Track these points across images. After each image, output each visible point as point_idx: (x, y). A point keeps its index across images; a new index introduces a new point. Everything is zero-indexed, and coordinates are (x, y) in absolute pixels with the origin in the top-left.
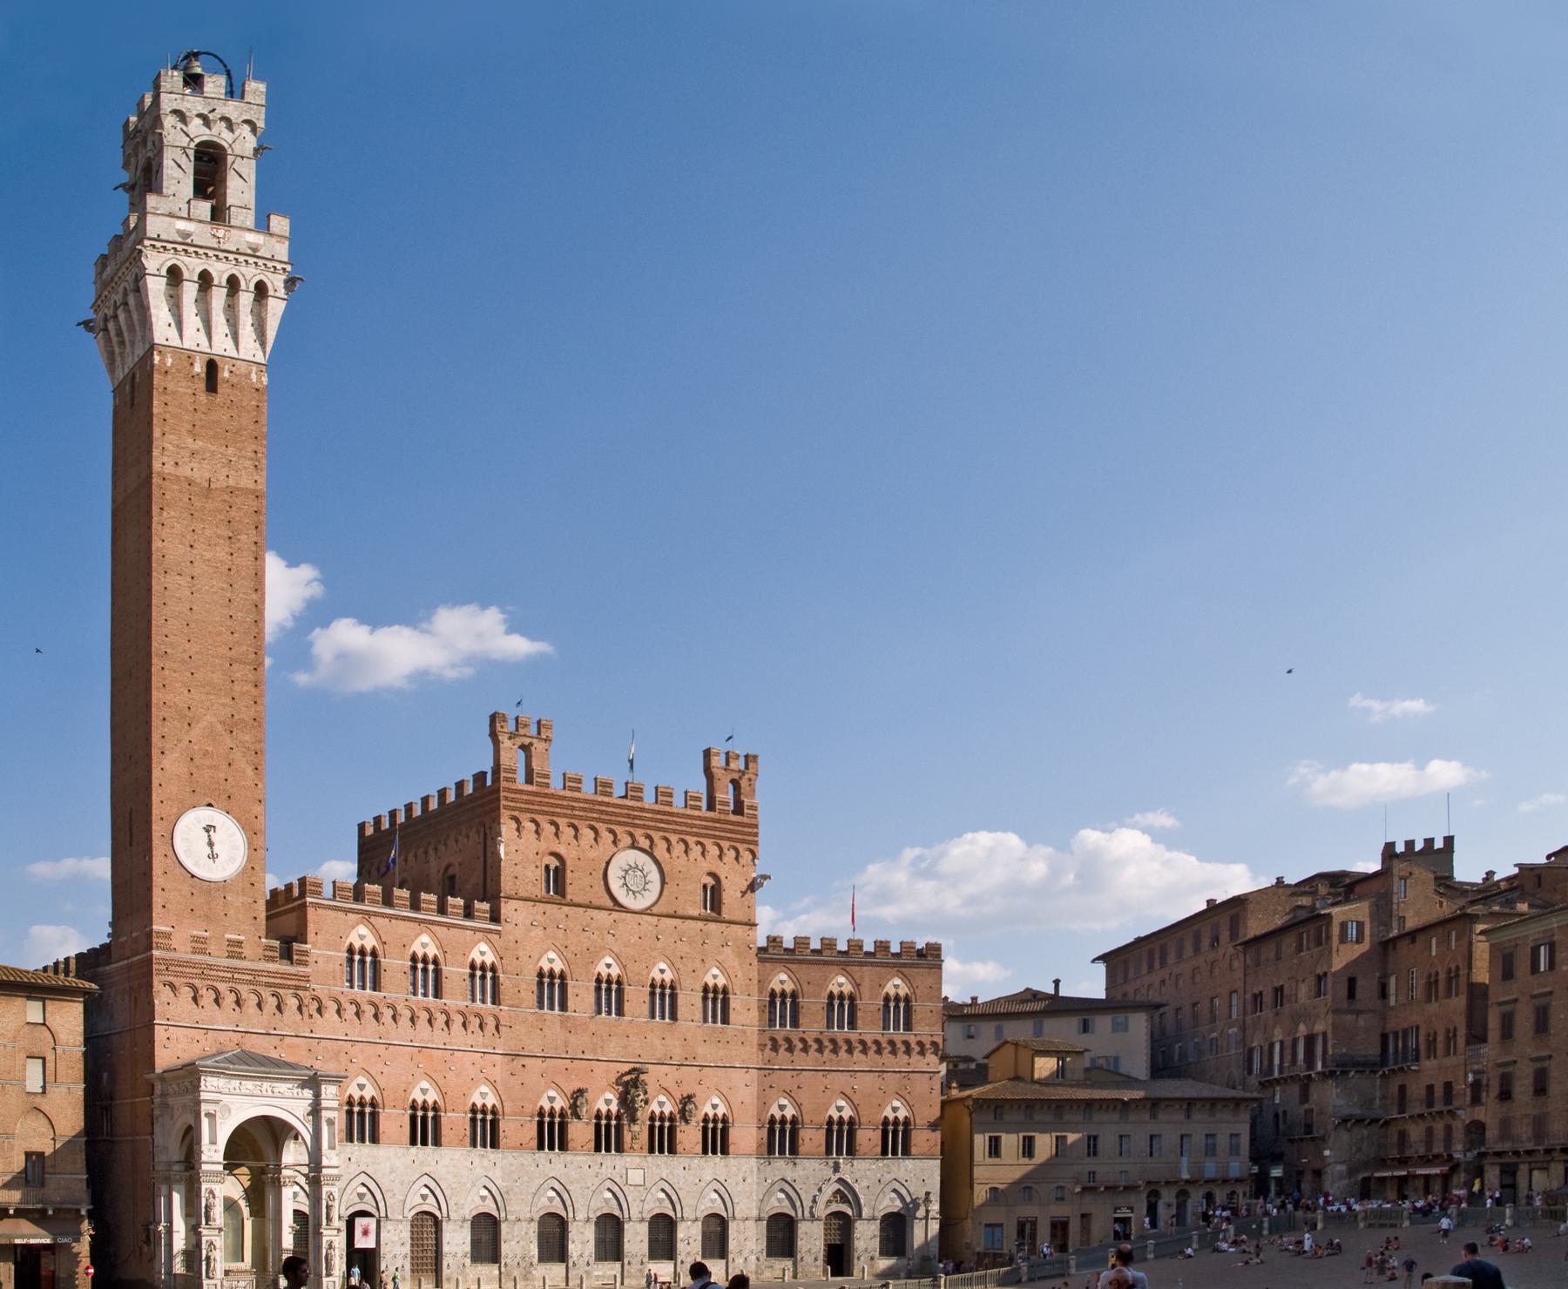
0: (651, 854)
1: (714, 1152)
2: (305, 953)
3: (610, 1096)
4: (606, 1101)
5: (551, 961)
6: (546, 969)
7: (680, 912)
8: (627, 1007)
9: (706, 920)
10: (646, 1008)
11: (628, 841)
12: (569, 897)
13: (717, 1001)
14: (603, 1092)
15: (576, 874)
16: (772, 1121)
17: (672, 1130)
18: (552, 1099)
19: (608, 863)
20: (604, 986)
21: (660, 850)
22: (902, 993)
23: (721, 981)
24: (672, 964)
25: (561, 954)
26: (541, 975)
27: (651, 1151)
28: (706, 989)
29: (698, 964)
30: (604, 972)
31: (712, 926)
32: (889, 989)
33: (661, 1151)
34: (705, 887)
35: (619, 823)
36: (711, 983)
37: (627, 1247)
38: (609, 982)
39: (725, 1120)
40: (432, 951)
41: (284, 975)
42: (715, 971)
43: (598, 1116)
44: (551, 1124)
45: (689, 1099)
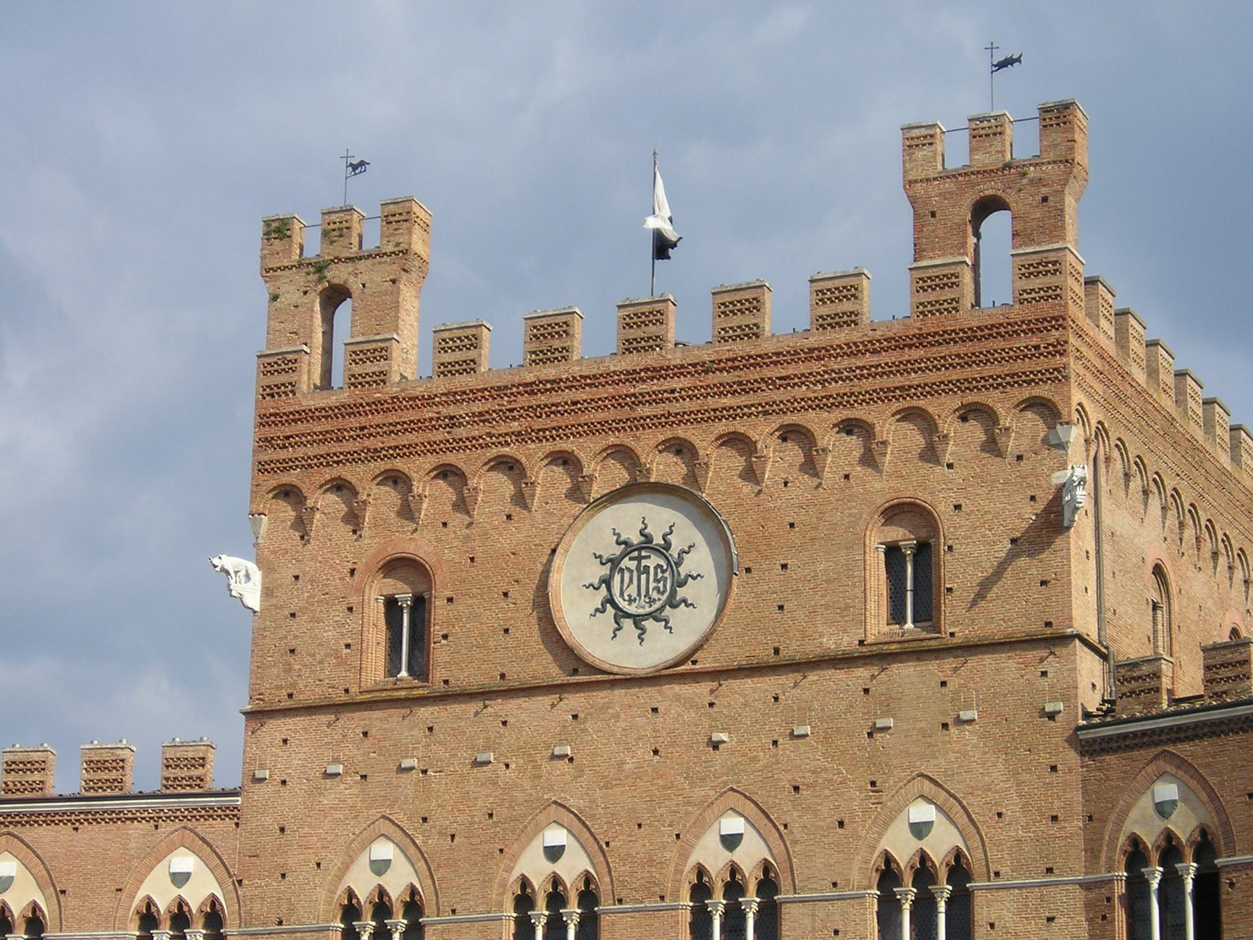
0: (683, 495)
7: (793, 649)
11: (618, 475)
15: (460, 607)
21: (721, 470)
24: (764, 817)
25: (407, 843)
28: (888, 875)
29: (855, 799)
30: (535, 868)
31: (905, 672)
34: (893, 552)
35: (592, 429)
36: (903, 849)
38: (556, 899)
42: (922, 812)
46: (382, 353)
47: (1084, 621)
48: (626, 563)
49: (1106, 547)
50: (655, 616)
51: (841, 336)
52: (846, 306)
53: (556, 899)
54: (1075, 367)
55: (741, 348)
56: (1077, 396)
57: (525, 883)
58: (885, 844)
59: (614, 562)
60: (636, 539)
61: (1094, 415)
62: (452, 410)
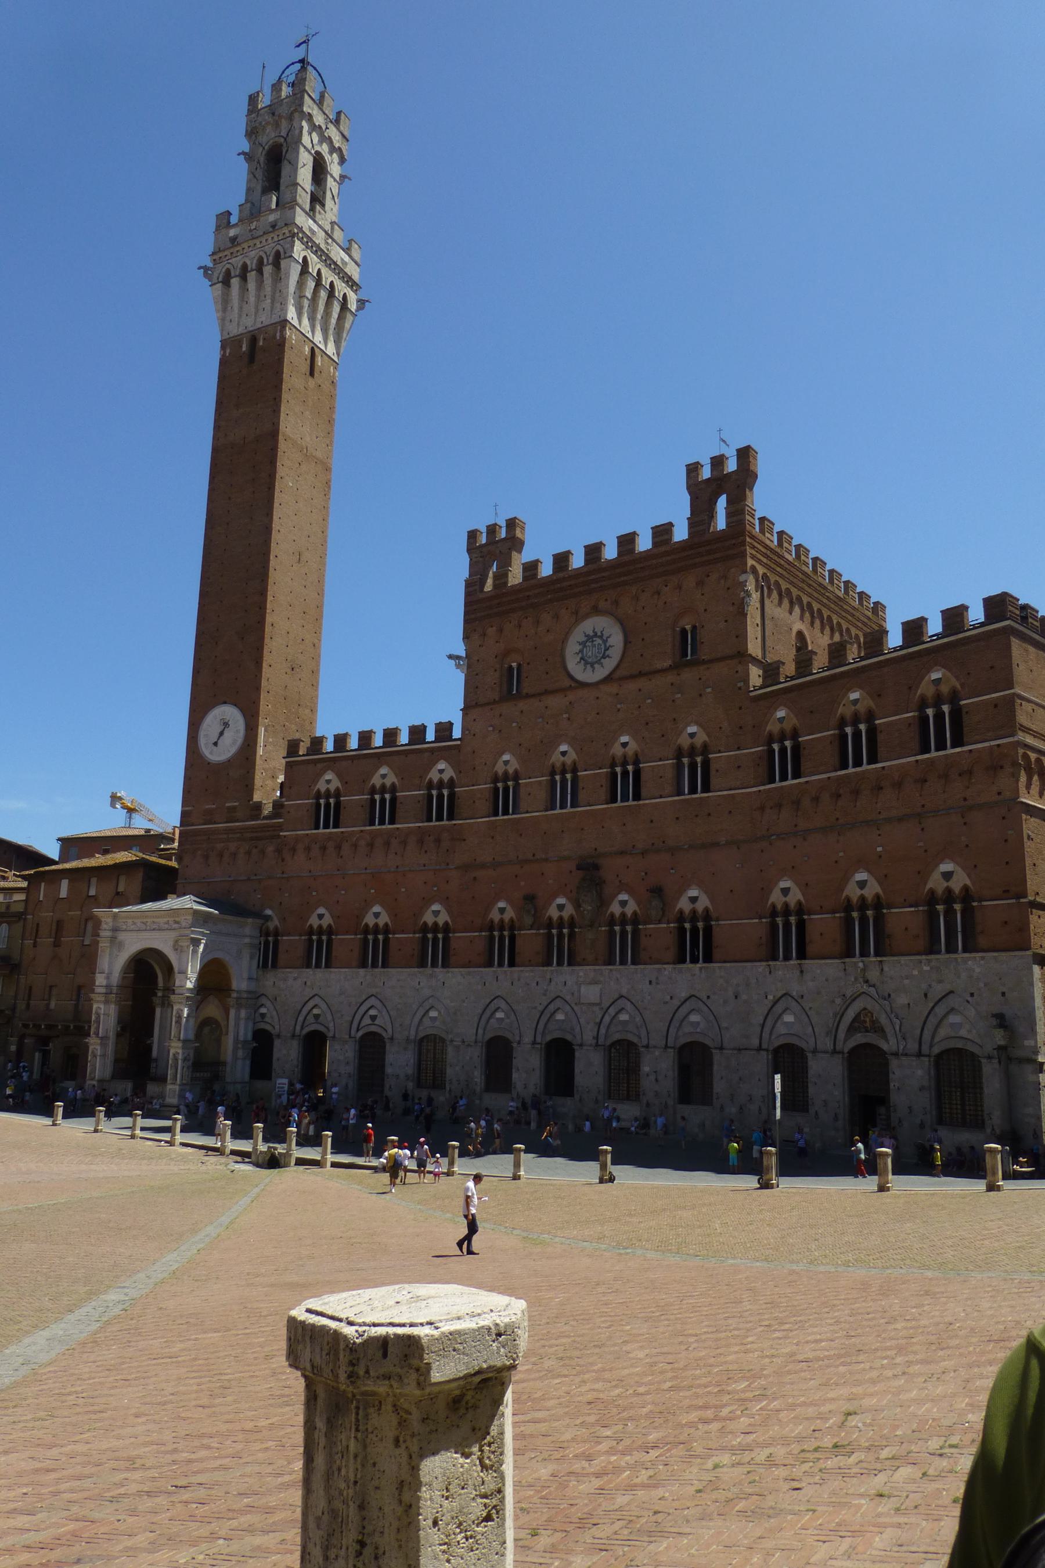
1: (695, 960)
2: (282, 806)
3: (561, 900)
4: (560, 907)
5: (506, 763)
6: (500, 772)
8: (582, 796)
9: (676, 667)
10: (603, 793)
12: (525, 691)
13: (696, 769)
14: (554, 896)
16: (774, 913)
17: (636, 933)
18: (502, 911)
19: (564, 641)
20: (558, 778)
22: (945, 689)
23: (702, 738)
26: (495, 779)
27: (610, 962)
28: (679, 754)
31: (688, 675)
32: (925, 689)
33: (623, 962)
36: (685, 742)
37: (579, 1079)
39: (707, 916)
40: (391, 779)
41: (263, 828)
43: (550, 925)
44: (502, 938)
45: (657, 891)
46: (505, 575)
47: (754, 648)
48: (589, 644)
49: (767, 622)
50: (599, 662)
51: (663, 549)
52: (666, 537)
53: (563, 772)
54: (749, 550)
55: (626, 558)
56: (750, 562)
57: (553, 767)
58: (679, 741)
59: (583, 644)
60: (591, 634)
61: (761, 570)
62: (527, 594)
